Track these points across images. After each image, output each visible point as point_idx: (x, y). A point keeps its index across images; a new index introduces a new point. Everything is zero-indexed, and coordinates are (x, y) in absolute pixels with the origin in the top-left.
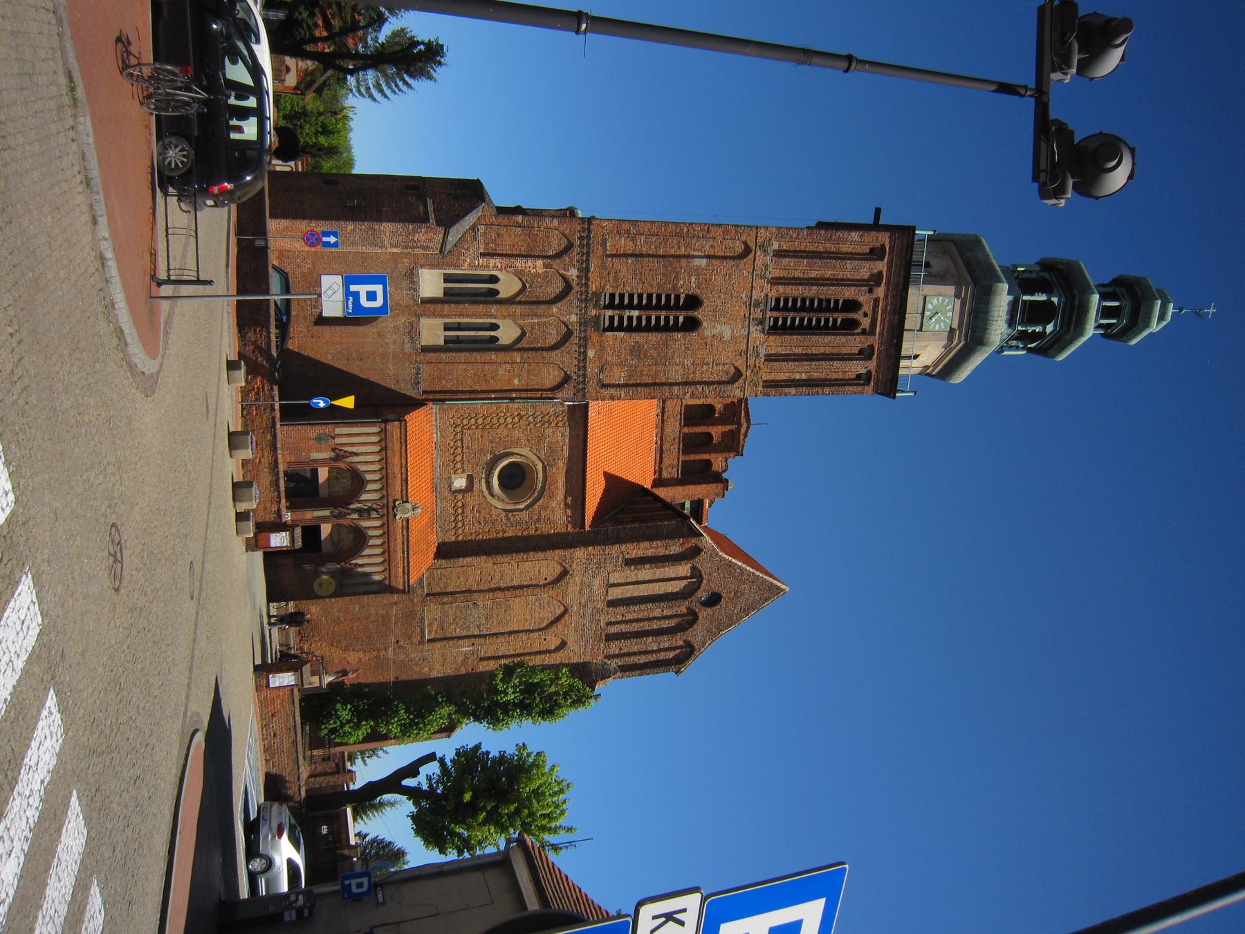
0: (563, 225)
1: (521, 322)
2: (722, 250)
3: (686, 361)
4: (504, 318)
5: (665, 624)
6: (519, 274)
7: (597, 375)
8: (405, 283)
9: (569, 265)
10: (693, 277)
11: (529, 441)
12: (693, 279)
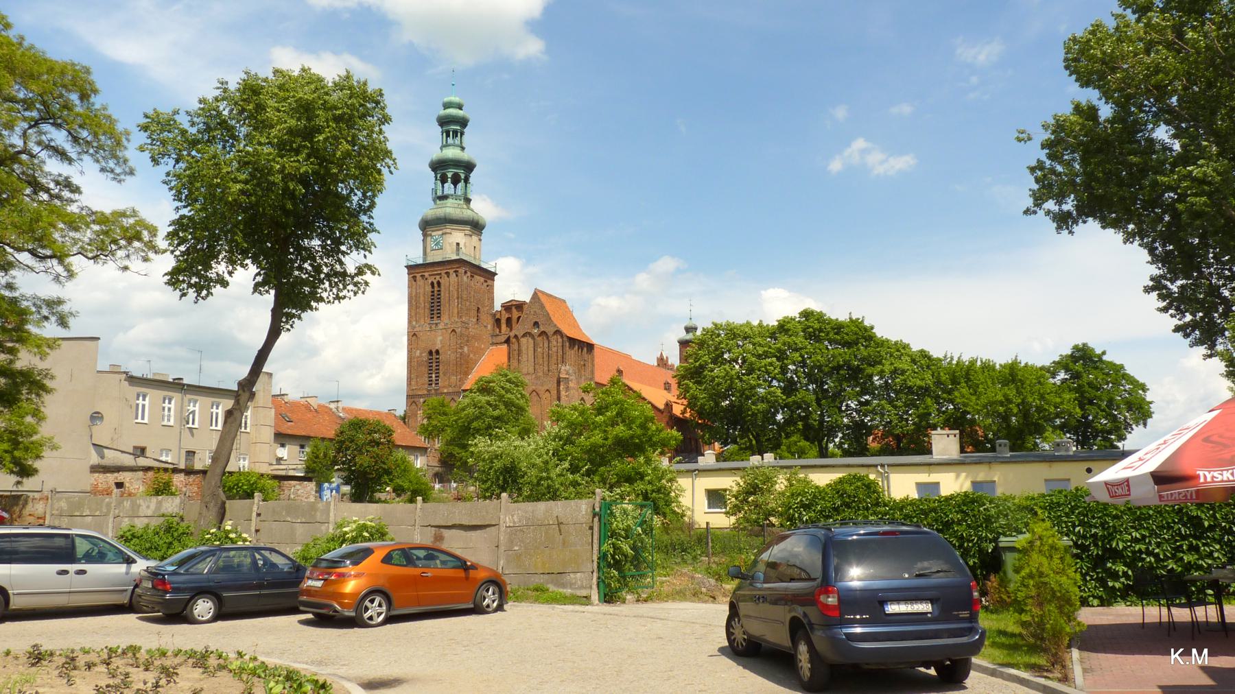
5: (546, 345)
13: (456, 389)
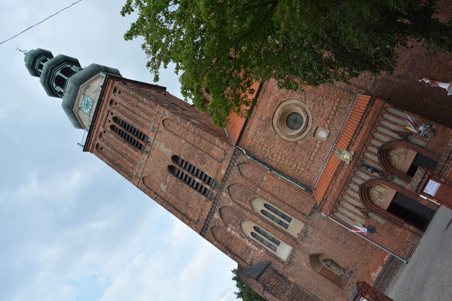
0: (212, 240)
1: (250, 208)
2: (154, 186)
3: (184, 142)
4: (257, 214)
6: (241, 231)
7: (224, 159)
8: (295, 261)
9: (217, 221)
10: (168, 181)
11: (274, 140)
12: (168, 180)
13: (230, 152)
